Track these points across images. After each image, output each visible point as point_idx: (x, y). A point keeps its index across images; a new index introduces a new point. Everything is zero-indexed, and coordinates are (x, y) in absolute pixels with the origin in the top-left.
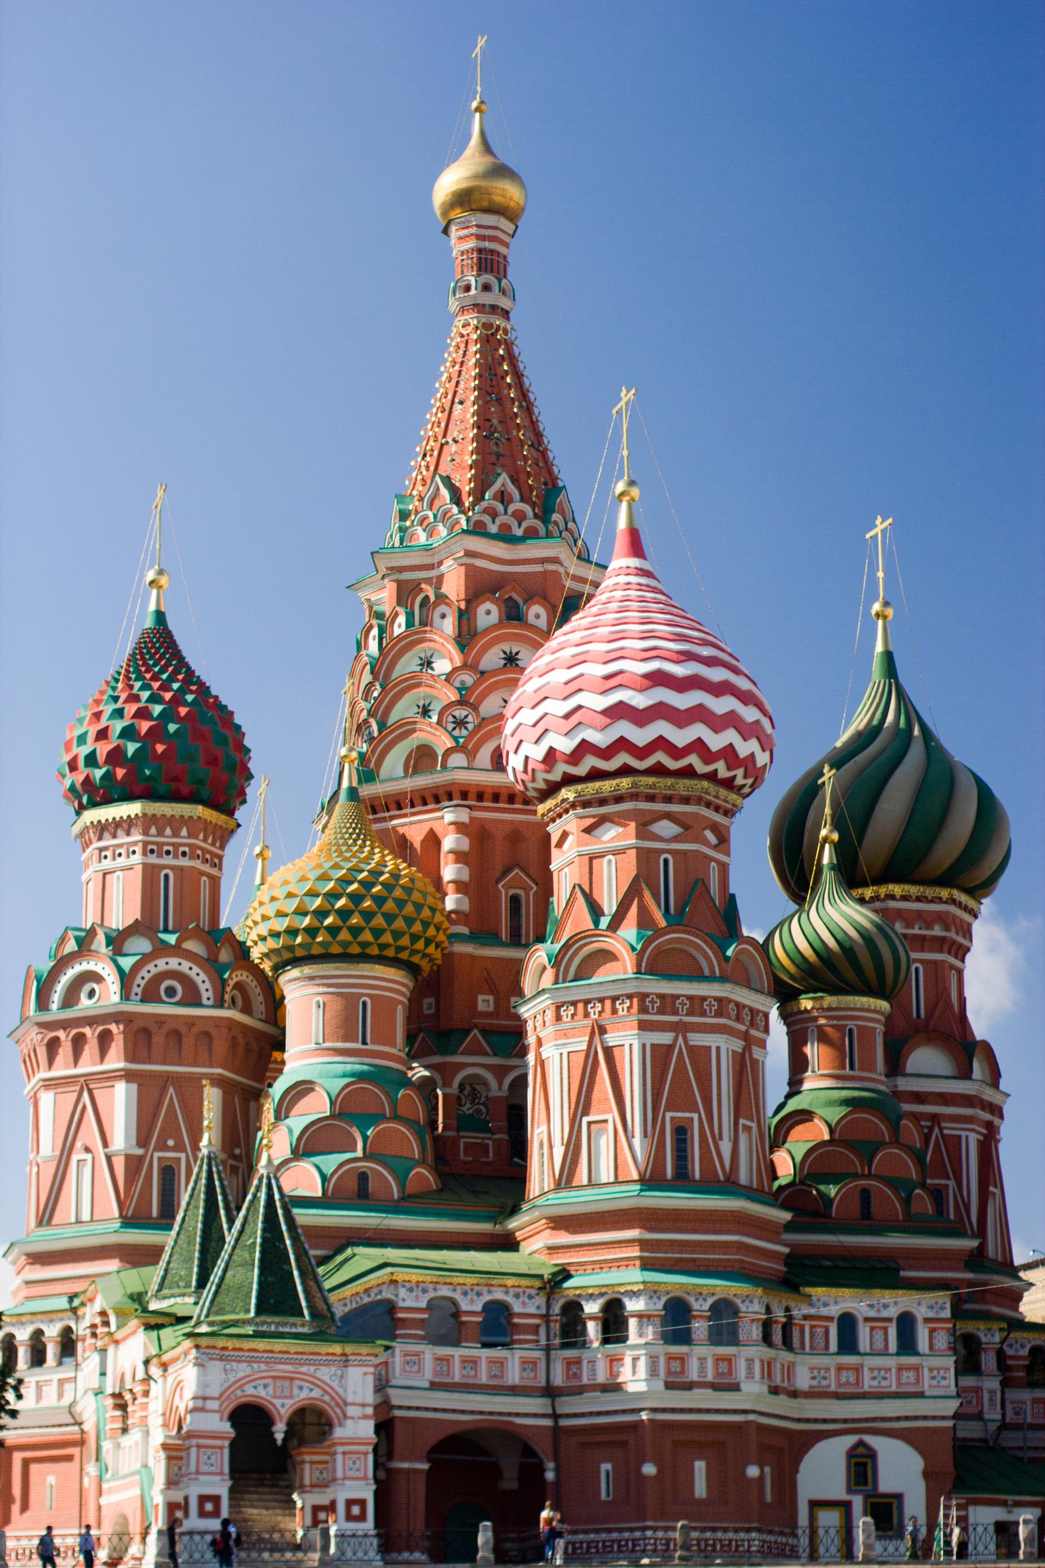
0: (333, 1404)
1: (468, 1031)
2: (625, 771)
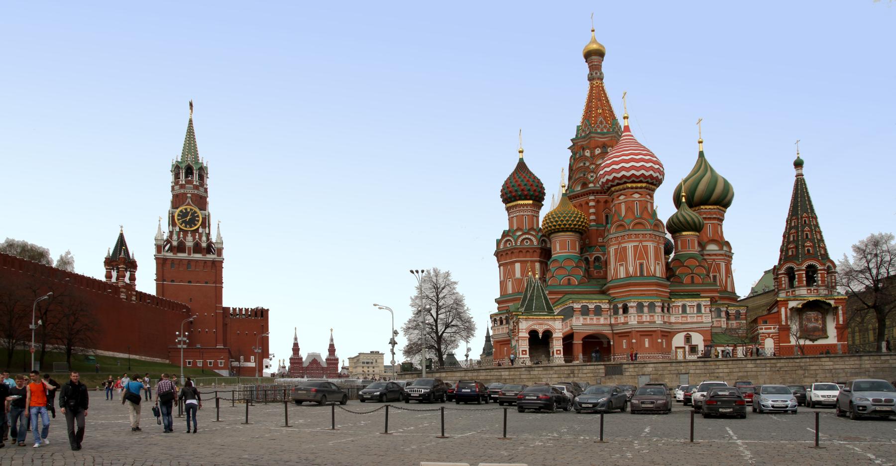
1: (596, 246)
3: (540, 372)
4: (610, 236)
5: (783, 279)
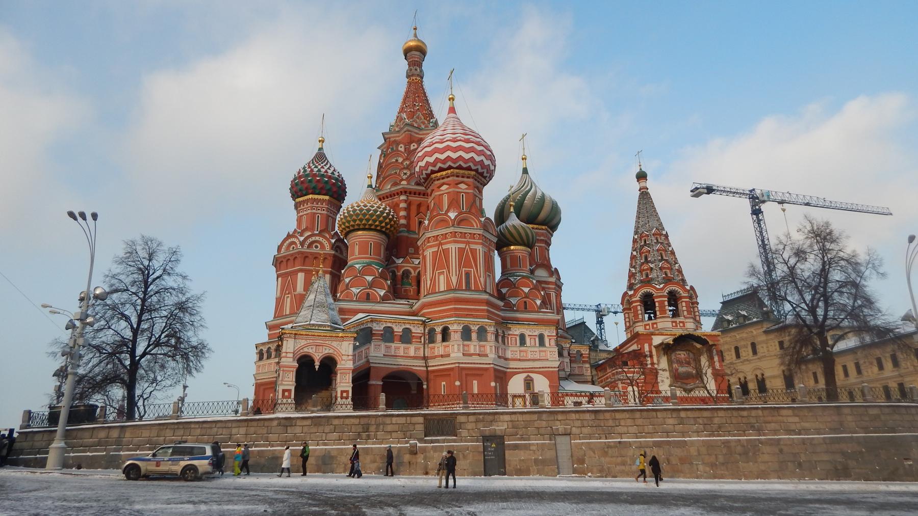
0: (338, 355)
2: (450, 168)
3: (305, 429)
4: (428, 235)
5: (639, 308)
